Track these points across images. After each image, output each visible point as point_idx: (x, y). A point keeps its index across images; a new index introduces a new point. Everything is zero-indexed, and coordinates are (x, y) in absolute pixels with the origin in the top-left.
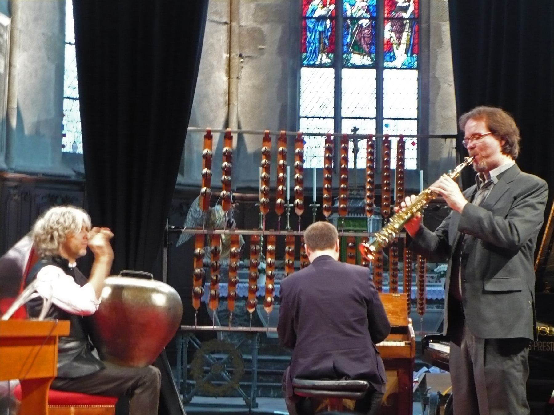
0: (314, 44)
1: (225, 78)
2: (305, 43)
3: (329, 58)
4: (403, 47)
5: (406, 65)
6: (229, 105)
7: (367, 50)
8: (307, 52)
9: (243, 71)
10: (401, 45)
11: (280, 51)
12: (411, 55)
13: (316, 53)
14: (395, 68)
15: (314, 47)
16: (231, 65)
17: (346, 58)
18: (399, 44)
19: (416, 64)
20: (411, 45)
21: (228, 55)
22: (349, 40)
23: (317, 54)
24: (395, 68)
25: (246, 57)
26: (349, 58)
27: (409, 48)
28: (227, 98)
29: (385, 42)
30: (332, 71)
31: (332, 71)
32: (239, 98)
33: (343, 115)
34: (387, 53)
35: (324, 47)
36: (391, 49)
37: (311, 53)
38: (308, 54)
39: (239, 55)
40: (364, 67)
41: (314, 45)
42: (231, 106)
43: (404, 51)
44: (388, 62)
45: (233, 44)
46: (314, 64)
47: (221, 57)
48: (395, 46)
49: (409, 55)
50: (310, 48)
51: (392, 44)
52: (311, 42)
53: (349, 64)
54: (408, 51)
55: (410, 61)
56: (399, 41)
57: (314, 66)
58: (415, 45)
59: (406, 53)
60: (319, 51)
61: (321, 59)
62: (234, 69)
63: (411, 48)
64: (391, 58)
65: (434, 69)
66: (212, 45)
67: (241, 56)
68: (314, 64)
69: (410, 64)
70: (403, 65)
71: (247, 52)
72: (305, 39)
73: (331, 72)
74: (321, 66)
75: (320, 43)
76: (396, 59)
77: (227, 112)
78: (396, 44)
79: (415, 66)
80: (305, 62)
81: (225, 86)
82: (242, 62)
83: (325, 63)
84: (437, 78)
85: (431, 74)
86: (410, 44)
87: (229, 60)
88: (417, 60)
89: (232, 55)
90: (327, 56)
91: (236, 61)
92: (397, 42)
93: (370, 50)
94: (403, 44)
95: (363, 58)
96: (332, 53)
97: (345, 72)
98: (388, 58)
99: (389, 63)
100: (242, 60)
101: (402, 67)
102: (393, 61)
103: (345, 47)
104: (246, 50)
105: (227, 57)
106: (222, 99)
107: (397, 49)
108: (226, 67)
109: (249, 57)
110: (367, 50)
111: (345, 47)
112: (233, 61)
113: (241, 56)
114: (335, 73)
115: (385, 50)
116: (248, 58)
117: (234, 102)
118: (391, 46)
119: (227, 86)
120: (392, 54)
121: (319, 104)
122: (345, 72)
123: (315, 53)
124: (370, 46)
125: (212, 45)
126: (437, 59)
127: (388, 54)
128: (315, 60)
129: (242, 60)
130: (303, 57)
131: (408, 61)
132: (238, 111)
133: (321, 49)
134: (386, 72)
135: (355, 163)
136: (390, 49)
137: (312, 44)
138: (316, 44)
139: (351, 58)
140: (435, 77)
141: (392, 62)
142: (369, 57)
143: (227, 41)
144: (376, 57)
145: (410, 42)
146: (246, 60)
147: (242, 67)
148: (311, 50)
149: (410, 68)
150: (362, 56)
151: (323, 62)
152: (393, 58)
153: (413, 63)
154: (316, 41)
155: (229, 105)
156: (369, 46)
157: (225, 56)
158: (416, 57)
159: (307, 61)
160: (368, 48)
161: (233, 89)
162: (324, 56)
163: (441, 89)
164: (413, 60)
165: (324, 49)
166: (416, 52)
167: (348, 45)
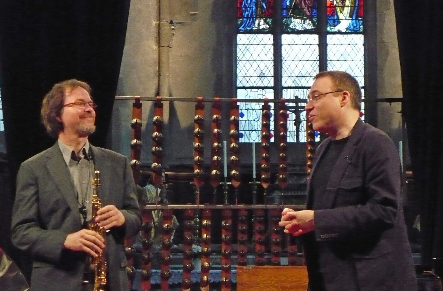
0: (250, 7)
1: (155, 47)
2: (241, 8)
3: (267, 23)
4: (347, 10)
5: (350, 30)
6: (159, 76)
7: (308, 14)
8: (243, 17)
9: (174, 38)
10: (346, 8)
11: (214, 17)
12: (357, 19)
13: (253, 18)
14: (340, 33)
15: (251, 12)
16: (161, 32)
17: (285, 22)
18: (343, 7)
19: (362, 28)
20: (356, 7)
21: (158, 22)
22: (288, 4)
23: (254, 19)
24: (340, 33)
25: (177, 23)
26: (289, 23)
27: (354, 11)
28: (157, 68)
29: (328, 5)
30: (271, 37)
31: (271, 37)
32: (171, 68)
33: (284, 84)
34: (330, 17)
35: (261, 11)
36: (334, 12)
37: (247, 18)
38: (245, 20)
39: (169, 21)
40: (305, 32)
41: (251, 10)
42: (162, 77)
43: (348, 15)
44: (331, 26)
45: (163, 10)
46: (252, 29)
47: (151, 24)
48: (338, 9)
49: (354, 18)
50: (247, 13)
51: (336, 6)
52: (248, 6)
53: (289, 29)
54: (353, 14)
55: (355, 25)
56: (342, 3)
57: (251, 32)
58: (360, 8)
59: (351, 16)
60: (256, 15)
61: (259, 25)
62: (163, 37)
63: (355, 10)
64: (334, 21)
65: (382, 33)
66: (140, 11)
67: (171, 22)
68: (252, 29)
69: (356, 28)
70: (347, 29)
71: (178, 19)
72: (241, 3)
73: (269, 39)
74: (260, 32)
75: (257, 8)
76: (339, 22)
77: (157, 85)
78: (339, 6)
79: (361, 30)
80: (241, 28)
81: (156, 56)
82: (173, 29)
83: (263, 29)
84: (385, 42)
85: (378, 40)
86: (355, 7)
87: (159, 27)
88: (363, 24)
89: (162, 22)
90: (266, 22)
91: (166, 28)
92: (340, 4)
93: (312, 13)
94: (347, 6)
95: (304, 23)
96: (270, 18)
97: (285, 39)
98: (331, 22)
99: (332, 27)
100: (173, 27)
101: (347, 32)
102: (337, 25)
103: (285, 11)
104: (177, 16)
105: (156, 24)
106: (153, 70)
107: (341, 12)
108: (156, 35)
109: (180, 23)
110: (308, 14)
111: (285, 11)
112: (163, 28)
113: (171, 22)
114: (274, 40)
115: (328, 13)
116: (179, 25)
117: (165, 73)
118: (334, 9)
119: (157, 56)
120: (336, 18)
121: (259, 72)
122: (285, 39)
123: (252, 18)
124: (311, 10)
125: (140, 11)
126: (384, 22)
127: (331, 18)
128: (252, 25)
129: (173, 27)
130: (239, 22)
131: (353, 25)
132: (169, 82)
133: (258, 14)
134: (329, 37)
135: (297, 136)
136: (333, 13)
137: (248, 9)
138: (252, 7)
139: (291, 22)
140: (383, 42)
141: (335, 26)
142: (310, 22)
143: (156, 7)
144: (318, 21)
145: (355, 4)
146: (178, 26)
147: (173, 34)
148: (248, 15)
149: (356, 33)
150: (303, 21)
151: (261, 27)
152: (337, 22)
153: (358, 27)
154: (253, 5)
155: (159, 76)
156: (310, 9)
157: (155, 22)
158: (361, 20)
159: (243, 27)
160: (309, 11)
161: (164, 59)
162: (262, 22)
163: (389, 55)
164: (358, 24)
165: (262, 13)
166: (362, 15)
167: (288, 8)
